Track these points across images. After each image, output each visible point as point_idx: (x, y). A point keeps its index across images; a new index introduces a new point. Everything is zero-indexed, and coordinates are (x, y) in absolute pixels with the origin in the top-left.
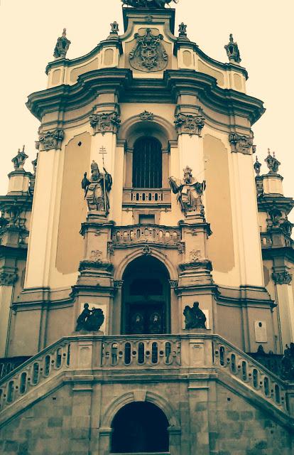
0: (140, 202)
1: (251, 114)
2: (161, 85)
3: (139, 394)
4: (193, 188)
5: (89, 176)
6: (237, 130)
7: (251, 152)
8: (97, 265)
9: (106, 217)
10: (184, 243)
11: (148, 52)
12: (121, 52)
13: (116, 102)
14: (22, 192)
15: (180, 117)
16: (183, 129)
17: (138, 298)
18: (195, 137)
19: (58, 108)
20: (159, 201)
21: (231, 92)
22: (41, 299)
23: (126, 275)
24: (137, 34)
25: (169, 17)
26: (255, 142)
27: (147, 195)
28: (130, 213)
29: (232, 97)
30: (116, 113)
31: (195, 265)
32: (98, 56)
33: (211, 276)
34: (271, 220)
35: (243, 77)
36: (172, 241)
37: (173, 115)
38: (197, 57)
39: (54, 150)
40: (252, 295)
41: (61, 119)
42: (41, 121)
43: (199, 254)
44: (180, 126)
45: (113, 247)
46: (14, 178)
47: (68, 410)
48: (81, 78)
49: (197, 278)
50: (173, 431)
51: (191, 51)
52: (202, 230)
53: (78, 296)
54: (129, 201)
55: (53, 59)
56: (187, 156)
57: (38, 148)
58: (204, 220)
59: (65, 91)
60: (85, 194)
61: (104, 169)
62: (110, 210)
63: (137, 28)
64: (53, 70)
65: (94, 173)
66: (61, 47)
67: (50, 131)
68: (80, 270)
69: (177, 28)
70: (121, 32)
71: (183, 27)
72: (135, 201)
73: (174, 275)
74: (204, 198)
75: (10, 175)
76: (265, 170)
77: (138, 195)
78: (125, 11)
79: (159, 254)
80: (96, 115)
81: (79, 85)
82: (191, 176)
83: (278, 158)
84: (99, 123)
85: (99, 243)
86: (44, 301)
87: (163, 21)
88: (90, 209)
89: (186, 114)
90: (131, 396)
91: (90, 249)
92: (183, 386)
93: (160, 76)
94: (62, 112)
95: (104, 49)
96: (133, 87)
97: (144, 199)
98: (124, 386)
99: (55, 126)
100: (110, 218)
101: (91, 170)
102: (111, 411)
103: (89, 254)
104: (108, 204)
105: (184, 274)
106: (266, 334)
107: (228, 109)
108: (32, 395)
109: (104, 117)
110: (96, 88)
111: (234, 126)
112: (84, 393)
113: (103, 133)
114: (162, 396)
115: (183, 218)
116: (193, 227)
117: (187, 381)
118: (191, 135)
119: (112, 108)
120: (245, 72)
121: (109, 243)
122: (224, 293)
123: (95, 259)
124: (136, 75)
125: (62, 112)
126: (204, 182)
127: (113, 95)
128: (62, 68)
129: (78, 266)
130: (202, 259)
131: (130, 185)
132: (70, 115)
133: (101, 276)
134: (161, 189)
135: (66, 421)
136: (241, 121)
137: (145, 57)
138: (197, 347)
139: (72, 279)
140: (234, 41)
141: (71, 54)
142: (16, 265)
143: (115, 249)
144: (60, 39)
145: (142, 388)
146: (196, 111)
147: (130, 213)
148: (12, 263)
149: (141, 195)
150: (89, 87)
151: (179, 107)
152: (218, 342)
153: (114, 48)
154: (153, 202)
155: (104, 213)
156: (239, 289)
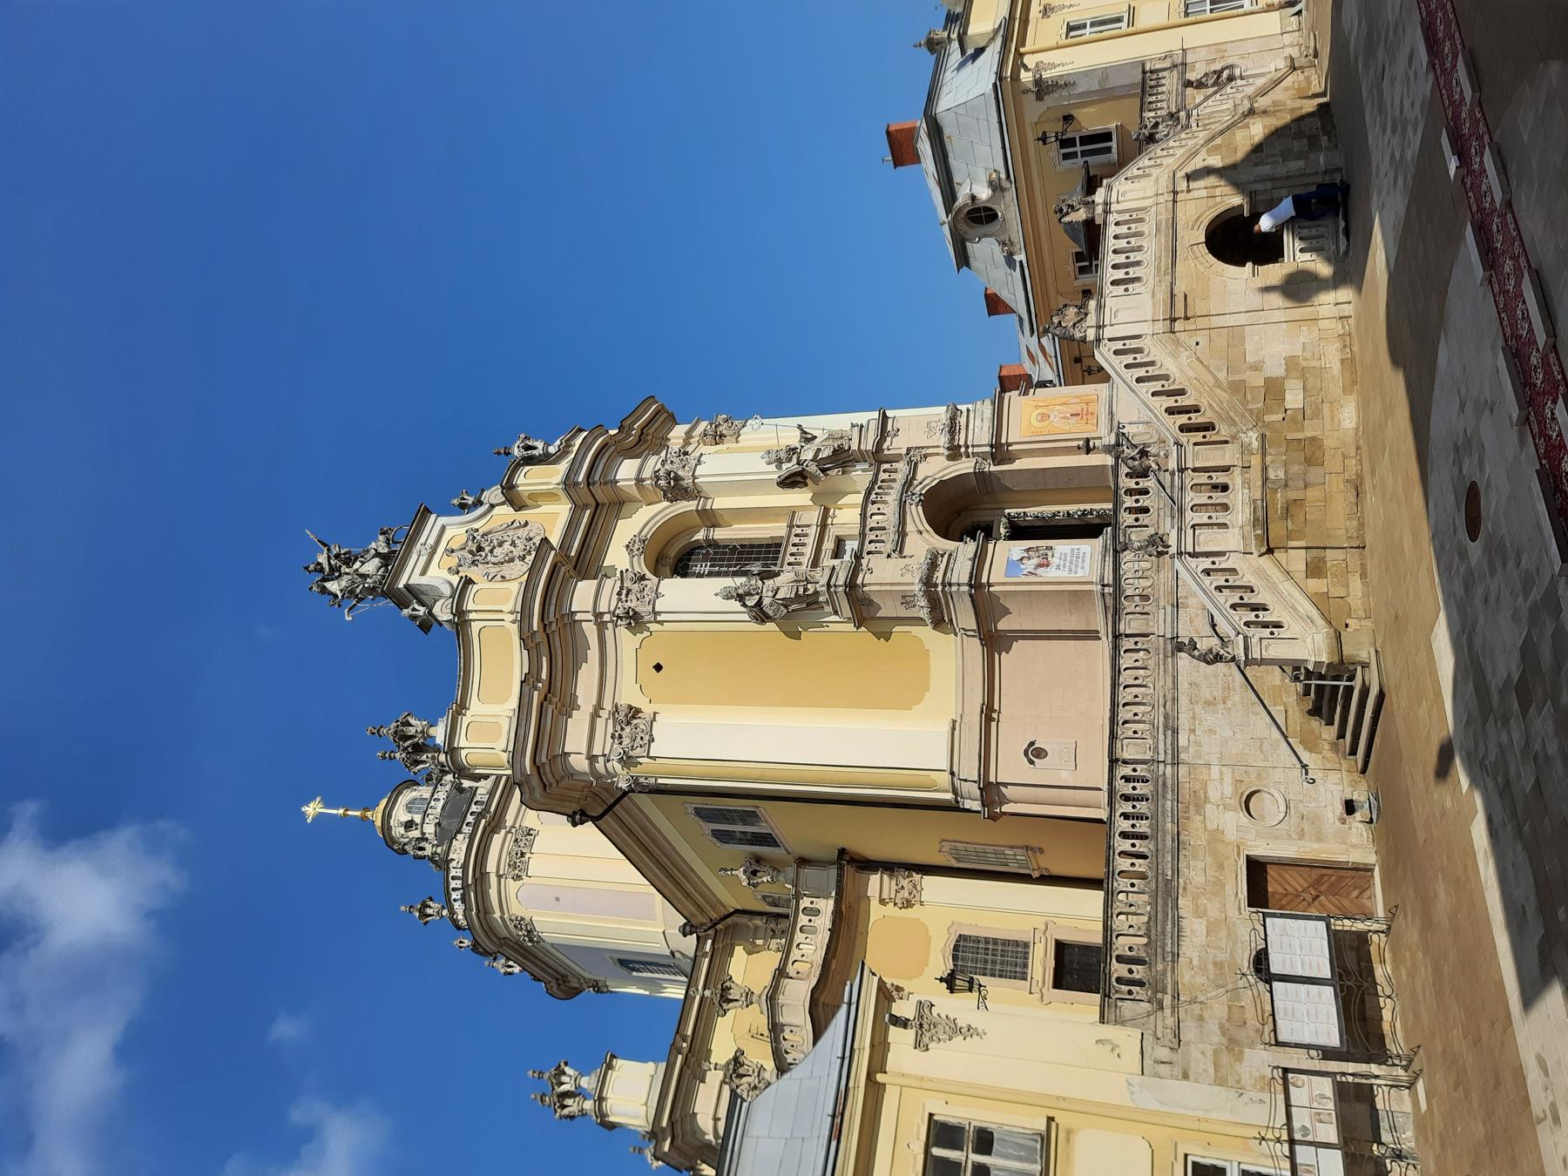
10: (909, 450)
11: (497, 551)
15: (661, 473)
20: (813, 532)
27: (794, 550)
49: (978, 422)
64: (461, 741)
67: (610, 730)
73: (965, 466)
84: (632, 605)
95: (470, 605)
99: (600, 723)
124: (555, 540)
128: (466, 720)
143: (901, 552)
154: (810, 541)
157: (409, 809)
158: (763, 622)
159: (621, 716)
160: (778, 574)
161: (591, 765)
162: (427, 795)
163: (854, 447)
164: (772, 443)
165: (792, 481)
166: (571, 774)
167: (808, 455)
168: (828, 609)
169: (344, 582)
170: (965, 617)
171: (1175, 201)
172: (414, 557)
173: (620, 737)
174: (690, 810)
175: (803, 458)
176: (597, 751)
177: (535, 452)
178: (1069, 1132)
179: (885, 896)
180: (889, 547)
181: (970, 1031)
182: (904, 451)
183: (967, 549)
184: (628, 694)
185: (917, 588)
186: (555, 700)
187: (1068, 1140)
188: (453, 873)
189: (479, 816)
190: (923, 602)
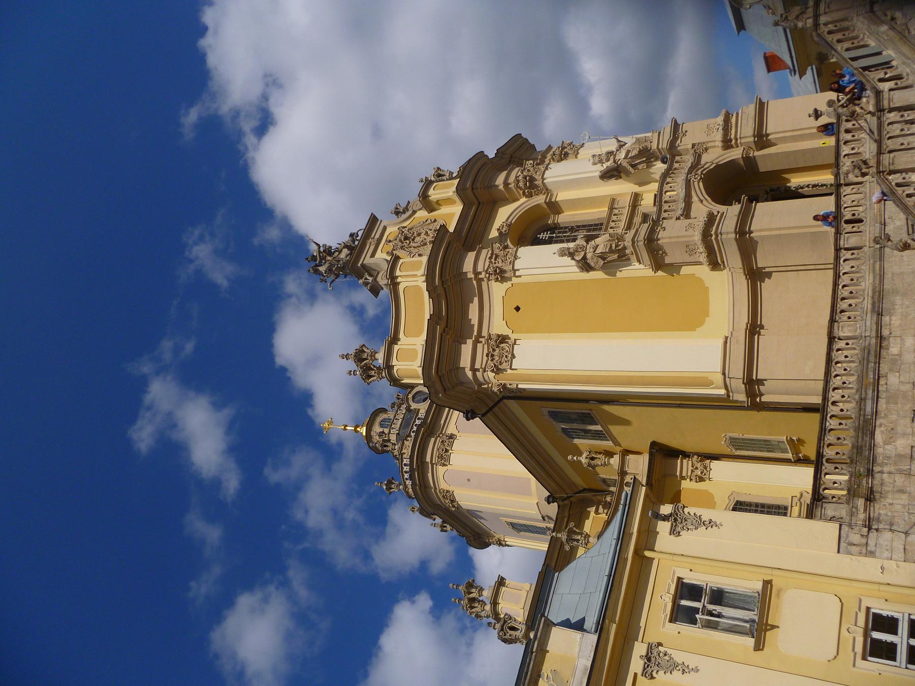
10: (693, 145)
11: (417, 239)
16: (538, 177)
20: (626, 211)
24: (388, 253)
43: (712, 126)
63: (379, 254)
64: (394, 362)
67: (486, 351)
73: (736, 154)
84: (500, 265)
95: (398, 273)
99: (479, 346)
121: (678, 219)
128: (396, 347)
153: (401, 261)
157: (381, 426)
158: (588, 271)
159: (492, 342)
160: (597, 236)
161: (474, 375)
162: (392, 417)
163: (654, 146)
164: (597, 151)
165: (613, 173)
166: (462, 382)
167: (621, 155)
168: (634, 258)
169: (327, 265)
170: (733, 257)
173: (492, 356)
174: (545, 411)
175: (617, 158)
176: (477, 366)
177: (444, 178)
178: (779, 591)
179: (684, 474)
180: (680, 212)
181: (711, 523)
182: (690, 146)
183: (734, 210)
184: (498, 327)
185: (697, 237)
187: (778, 595)
188: (405, 461)
189: (419, 427)
190: (702, 249)
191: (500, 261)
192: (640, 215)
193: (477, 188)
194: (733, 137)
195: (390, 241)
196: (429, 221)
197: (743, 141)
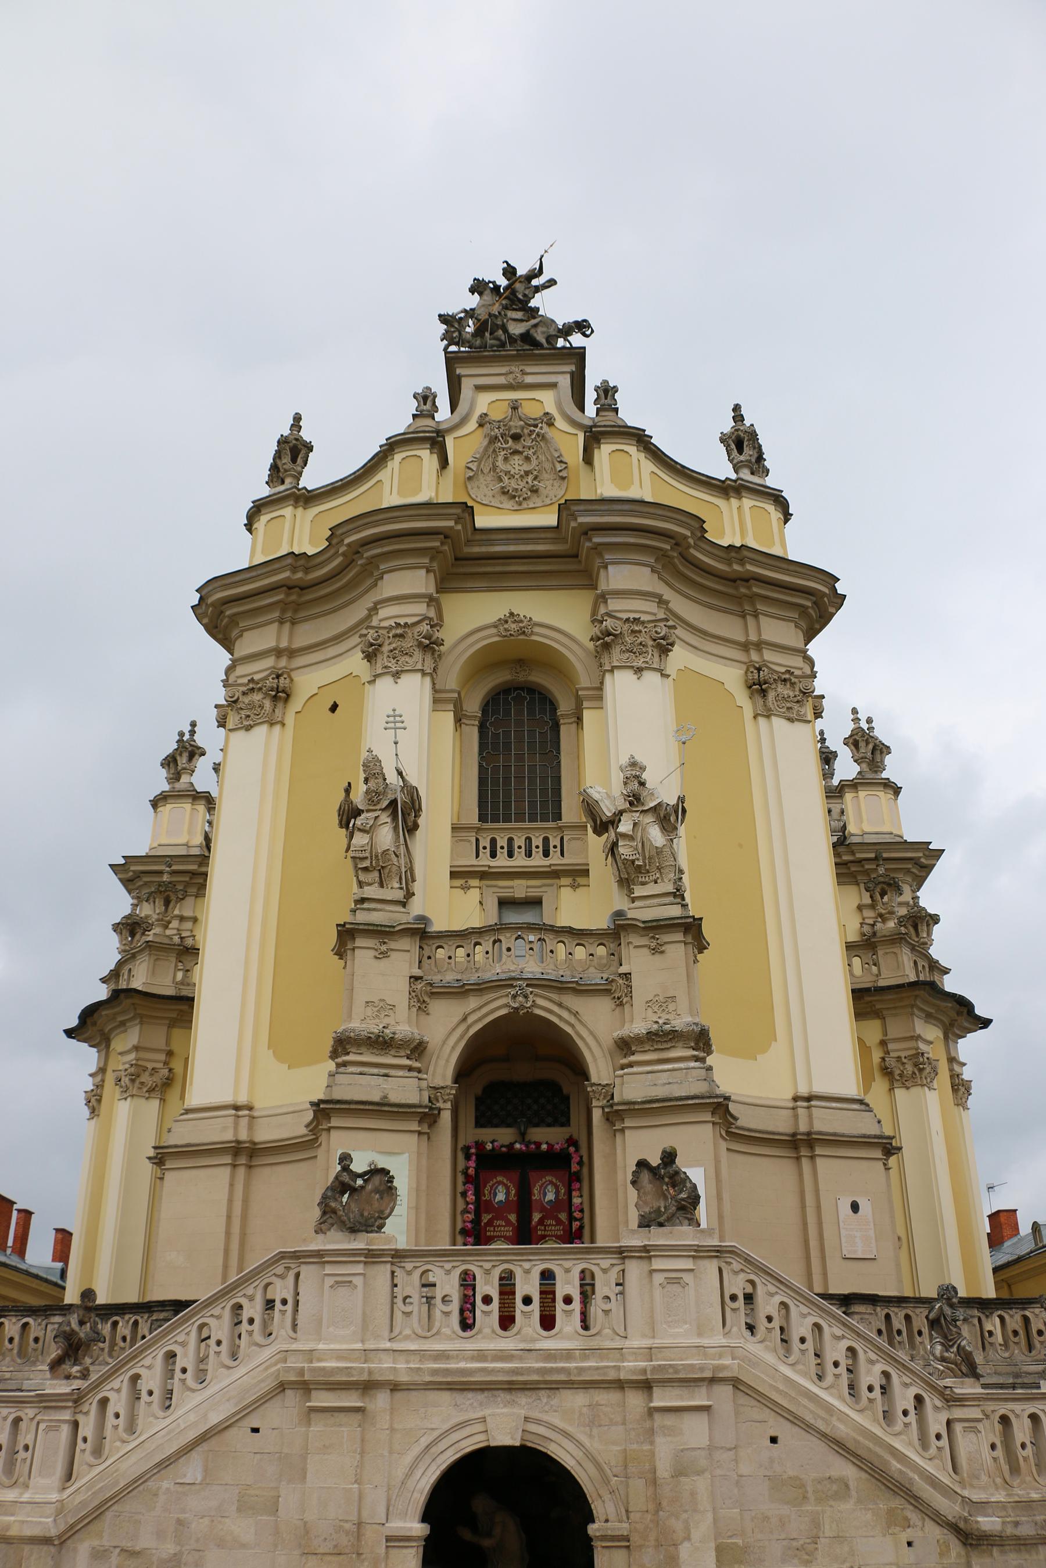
0: (502, 861)
1: (803, 611)
2: (555, 541)
3: (503, 1426)
4: (649, 819)
5: (358, 797)
6: (769, 655)
7: (810, 716)
8: (382, 1043)
9: (404, 904)
10: (627, 976)
11: (517, 460)
12: (444, 463)
13: (432, 590)
14: (187, 845)
15: (609, 623)
16: (617, 656)
17: (501, 1137)
18: (651, 678)
19: (277, 614)
20: (555, 859)
21: (746, 553)
22: (229, 1136)
23: (463, 1073)
25: (573, 368)
26: (819, 686)
27: (519, 841)
28: (474, 895)
29: (749, 567)
30: (431, 619)
31: (661, 1038)
32: (383, 475)
33: (710, 1069)
34: (873, 906)
35: (775, 515)
36: (592, 970)
37: (587, 617)
38: (649, 466)
39: (264, 728)
40: (826, 1121)
41: (284, 644)
42: (230, 650)
44: (607, 646)
45: (425, 992)
46: (166, 809)
47: (296, 1469)
48: (335, 533)
50: (604, 1538)
51: (632, 449)
52: (679, 936)
53: (329, 1130)
54: (468, 860)
55: (265, 491)
56: (632, 729)
57: (222, 724)
58: (685, 906)
59: (294, 569)
60: (345, 841)
61: (400, 773)
62: (417, 887)
63: (484, 403)
64: (264, 519)
65: (372, 784)
66: (286, 459)
67: (256, 677)
68: (334, 1055)
69: (590, 396)
70: (443, 413)
71: (607, 391)
72: (485, 861)
73: (600, 1068)
74: (682, 846)
75: (155, 803)
76: (846, 768)
77: (493, 841)
78: (451, 361)
79: (555, 1009)
80: (377, 628)
81: (332, 551)
82: (642, 784)
83: (881, 734)
84: (386, 648)
85: (383, 980)
86: (238, 1142)
87: (552, 379)
88: (361, 884)
89: (625, 616)
90: (480, 1427)
91: (361, 997)
92: (635, 1400)
93: (549, 518)
94: (287, 625)
95: (398, 457)
96: (476, 550)
97: (510, 855)
98: (458, 1397)
99: (269, 662)
100: (417, 907)
101: (362, 776)
102: (418, 1473)
103: (359, 1008)
104: (411, 870)
105: (630, 1065)
106: (872, 1233)
107: (738, 599)
108: (192, 1417)
109: (399, 631)
110: (373, 557)
111: (759, 646)
112: (341, 1417)
113: (397, 675)
114: (570, 1429)
115: (620, 903)
116: (656, 928)
117: (646, 1386)
118: (639, 671)
119: (420, 609)
120: (779, 501)
122: (747, 1119)
123: (373, 1027)
124: (482, 521)
125: (287, 625)
126: (681, 799)
127: (423, 572)
128: (288, 511)
129: (328, 1045)
130: (681, 1022)
131: (472, 817)
132: (306, 634)
133: (392, 1072)
134: (560, 823)
135: (289, 1499)
136: (778, 630)
137: (507, 473)
138: (677, 1281)
139: (313, 1081)
140: (747, 423)
141: (312, 478)
142: (168, 1043)
144: (282, 442)
145: (512, 1403)
146: (651, 606)
147: (474, 895)
148: (157, 1037)
149: (502, 842)
150: (364, 550)
151: (603, 598)
152: (736, 1266)
154: (538, 861)
155: (399, 895)
156: (791, 1104)
159: (271, 682)
171: (620, 1385)
172: (504, 370)
182: (623, 970)
186: (293, 597)
191: (394, 645)
192: (533, 893)
193: (590, 540)
194: (633, 1058)
195: (515, 408)
196: (559, 467)
197: (618, 1081)
